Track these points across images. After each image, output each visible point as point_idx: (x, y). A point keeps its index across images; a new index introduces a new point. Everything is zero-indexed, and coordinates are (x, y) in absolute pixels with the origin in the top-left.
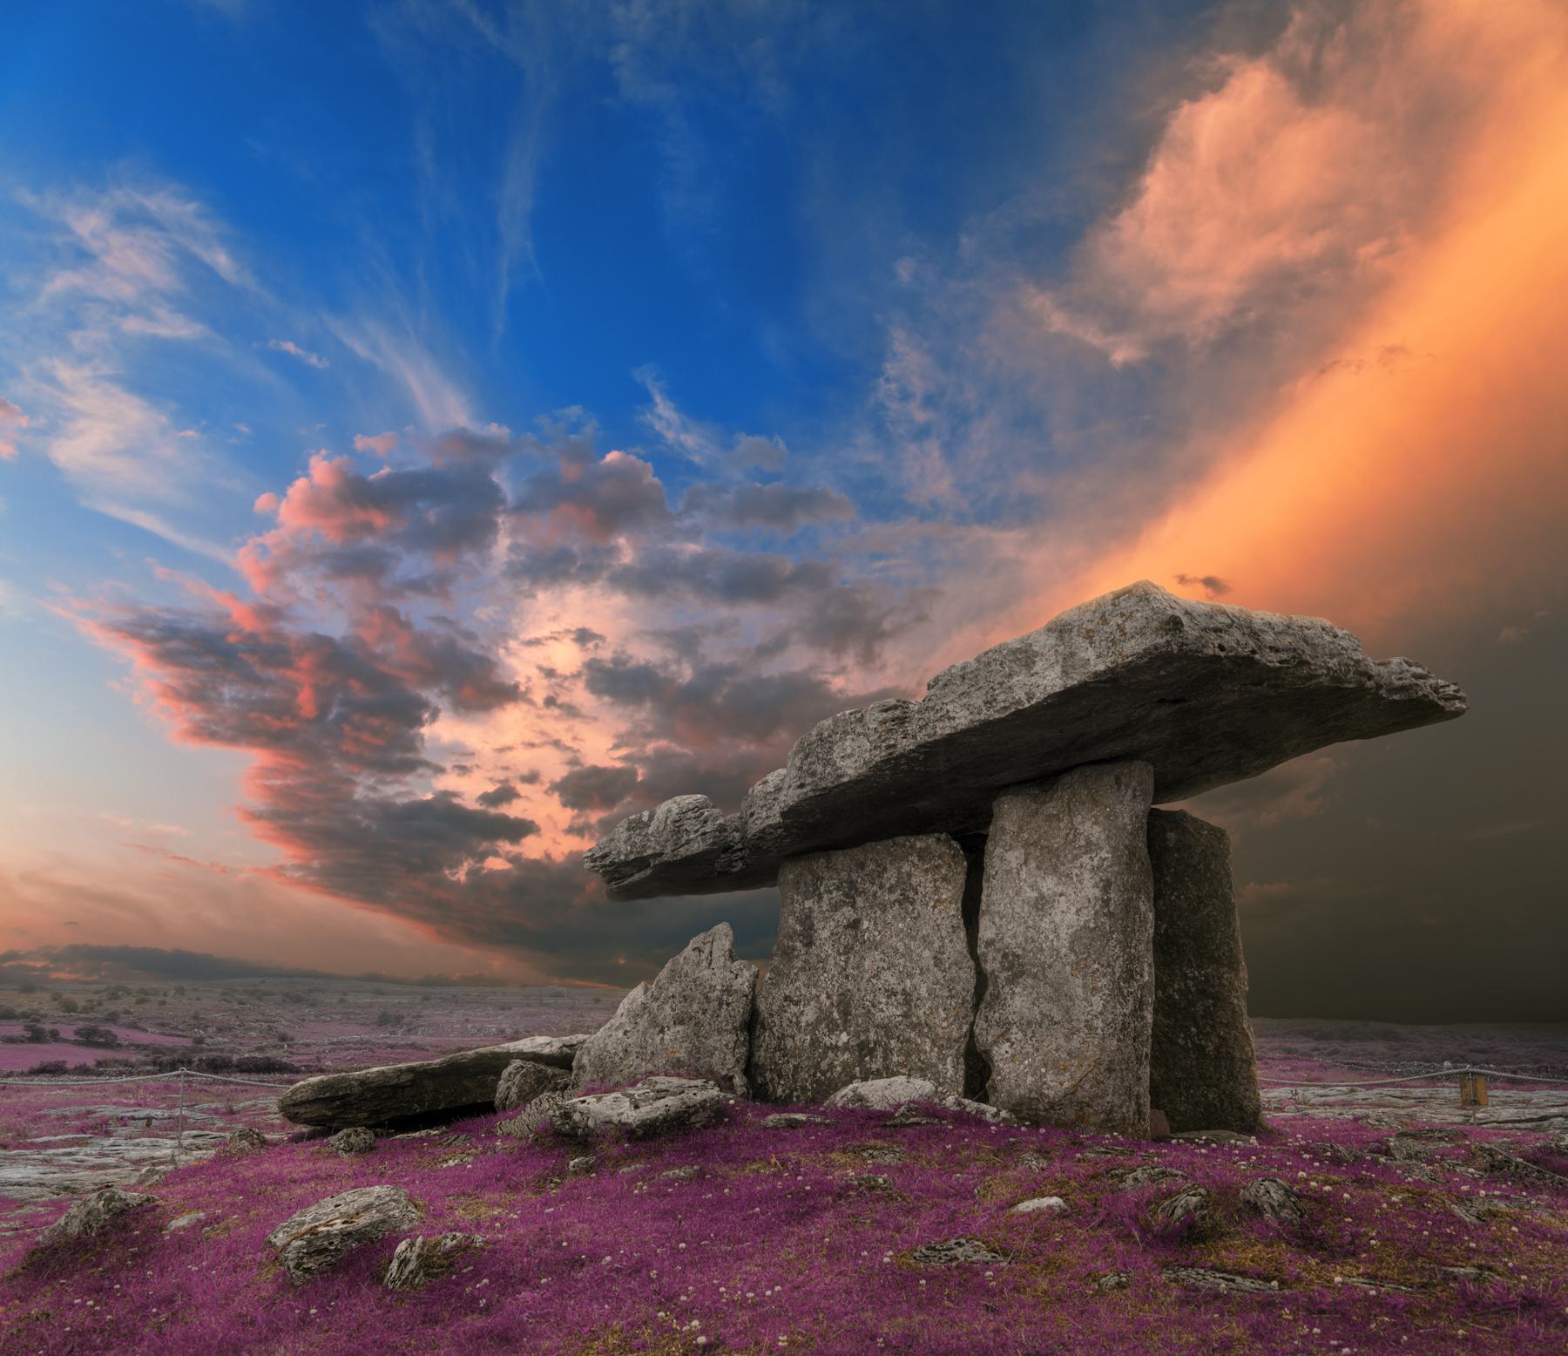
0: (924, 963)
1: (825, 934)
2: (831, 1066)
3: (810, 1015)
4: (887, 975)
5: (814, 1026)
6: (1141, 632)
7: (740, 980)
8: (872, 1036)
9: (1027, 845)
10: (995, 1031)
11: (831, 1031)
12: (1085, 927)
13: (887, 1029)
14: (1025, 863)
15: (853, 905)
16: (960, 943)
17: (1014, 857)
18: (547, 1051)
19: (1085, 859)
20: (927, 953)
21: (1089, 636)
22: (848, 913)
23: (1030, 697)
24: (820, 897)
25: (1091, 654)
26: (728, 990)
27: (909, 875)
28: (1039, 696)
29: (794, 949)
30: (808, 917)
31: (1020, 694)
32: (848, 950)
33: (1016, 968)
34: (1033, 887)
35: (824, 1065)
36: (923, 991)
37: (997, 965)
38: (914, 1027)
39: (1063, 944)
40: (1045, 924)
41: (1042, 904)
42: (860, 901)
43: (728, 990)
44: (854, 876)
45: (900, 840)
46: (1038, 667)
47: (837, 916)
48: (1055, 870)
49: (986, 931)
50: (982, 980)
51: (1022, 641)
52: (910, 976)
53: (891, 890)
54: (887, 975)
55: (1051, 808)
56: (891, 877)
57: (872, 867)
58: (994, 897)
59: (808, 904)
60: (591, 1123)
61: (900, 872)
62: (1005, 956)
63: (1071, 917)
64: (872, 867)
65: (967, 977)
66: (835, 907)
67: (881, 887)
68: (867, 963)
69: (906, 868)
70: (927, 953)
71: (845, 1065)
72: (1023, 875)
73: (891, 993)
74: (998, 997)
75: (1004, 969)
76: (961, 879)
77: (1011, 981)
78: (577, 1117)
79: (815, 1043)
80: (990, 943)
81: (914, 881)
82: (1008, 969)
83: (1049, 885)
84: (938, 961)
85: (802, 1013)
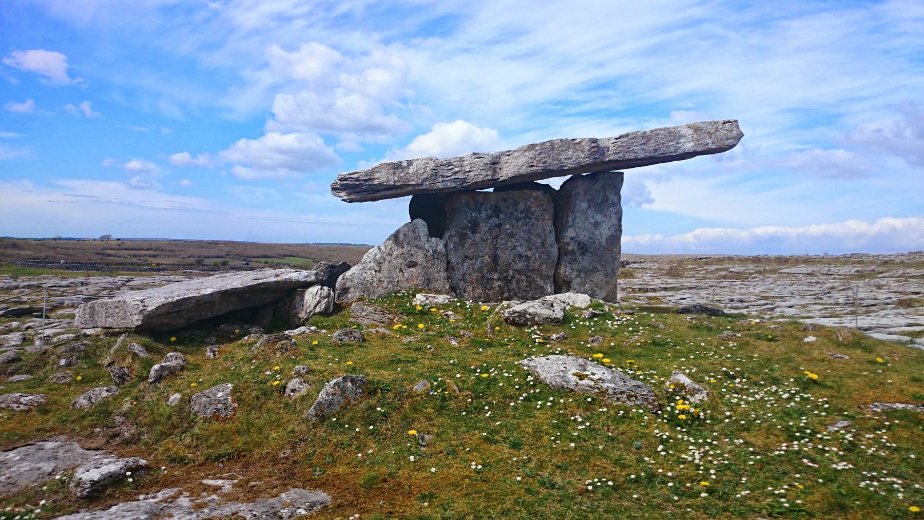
0: (538, 245)
1: (486, 229)
3: (478, 265)
4: (519, 248)
5: (480, 270)
8: (511, 272)
9: (589, 201)
10: (575, 273)
11: (490, 272)
12: (612, 235)
13: (519, 272)
14: (589, 207)
15: (498, 217)
16: (553, 238)
17: (584, 205)
19: (612, 209)
20: (539, 240)
22: (495, 220)
24: (480, 212)
25: (709, 141)
27: (530, 207)
28: (680, 151)
29: (467, 234)
30: (475, 221)
32: (497, 237)
33: (583, 249)
34: (593, 218)
36: (537, 256)
37: (575, 248)
38: (531, 271)
39: (604, 241)
40: (597, 233)
41: (596, 225)
42: (502, 216)
44: (499, 204)
45: (525, 191)
46: (681, 141)
47: (491, 221)
48: (601, 212)
49: (571, 233)
50: (562, 252)
51: (674, 128)
52: (530, 250)
53: (521, 212)
54: (519, 248)
55: (597, 187)
56: (521, 206)
57: (511, 201)
58: (577, 220)
59: (474, 214)
61: (525, 204)
62: (579, 244)
63: (606, 231)
64: (511, 201)
65: (555, 251)
66: (489, 217)
67: (516, 210)
68: (509, 244)
69: (529, 204)
70: (539, 240)
71: (499, 286)
72: (589, 212)
73: (521, 256)
74: (575, 260)
75: (578, 249)
76: (552, 211)
77: (583, 254)
79: (483, 277)
80: (572, 238)
81: (532, 210)
82: (582, 249)
83: (599, 217)
84: (543, 244)
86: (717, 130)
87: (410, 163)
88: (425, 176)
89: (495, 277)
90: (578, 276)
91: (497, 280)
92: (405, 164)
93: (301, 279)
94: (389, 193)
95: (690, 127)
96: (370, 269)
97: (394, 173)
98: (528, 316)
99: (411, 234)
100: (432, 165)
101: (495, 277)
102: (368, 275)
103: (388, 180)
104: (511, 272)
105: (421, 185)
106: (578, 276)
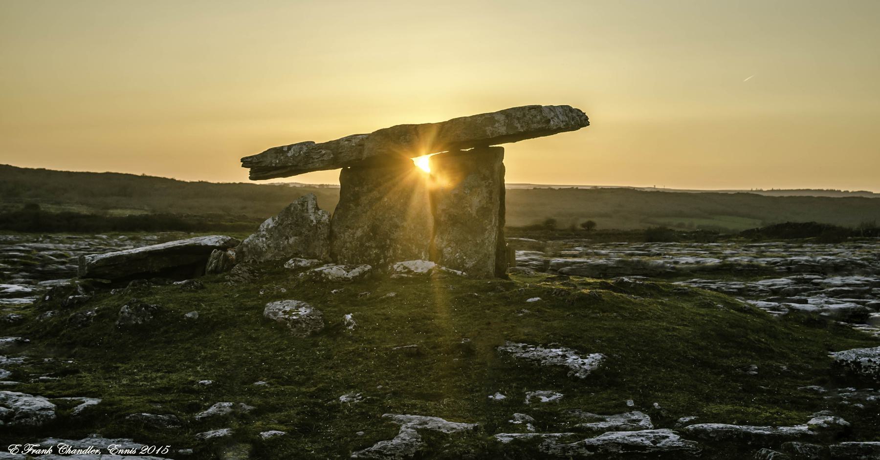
1: (366, 202)
2: (370, 255)
5: (361, 237)
6: (538, 123)
7: (324, 218)
10: (445, 243)
11: (369, 241)
12: (482, 207)
18: (218, 244)
21: (518, 119)
23: (492, 134)
25: (519, 125)
26: (319, 222)
28: (496, 135)
31: (488, 133)
35: (366, 254)
39: (474, 213)
43: (319, 222)
46: (497, 125)
60: (330, 278)
62: (450, 215)
78: (323, 275)
79: (362, 245)
85: (355, 233)
86: (524, 115)
87: (290, 147)
88: (299, 158)
89: (374, 245)
90: (448, 245)
91: (375, 248)
92: (286, 149)
93: (209, 244)
94: (275, 172)
95: (502, 112)
96: (262, 237)
97: (277, 157)
98: (323, 275)
99: (299, 207)
100: (305, 149)
101: (374, 245)
102: (261, 243)
103: (271, 163)
104: (388, 241)
105: (297, 166)
106: (448, 245)
